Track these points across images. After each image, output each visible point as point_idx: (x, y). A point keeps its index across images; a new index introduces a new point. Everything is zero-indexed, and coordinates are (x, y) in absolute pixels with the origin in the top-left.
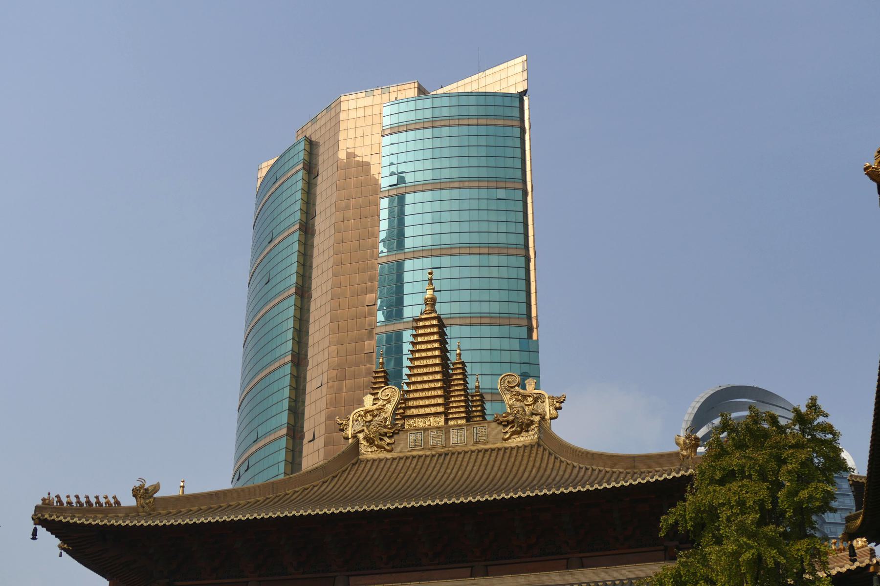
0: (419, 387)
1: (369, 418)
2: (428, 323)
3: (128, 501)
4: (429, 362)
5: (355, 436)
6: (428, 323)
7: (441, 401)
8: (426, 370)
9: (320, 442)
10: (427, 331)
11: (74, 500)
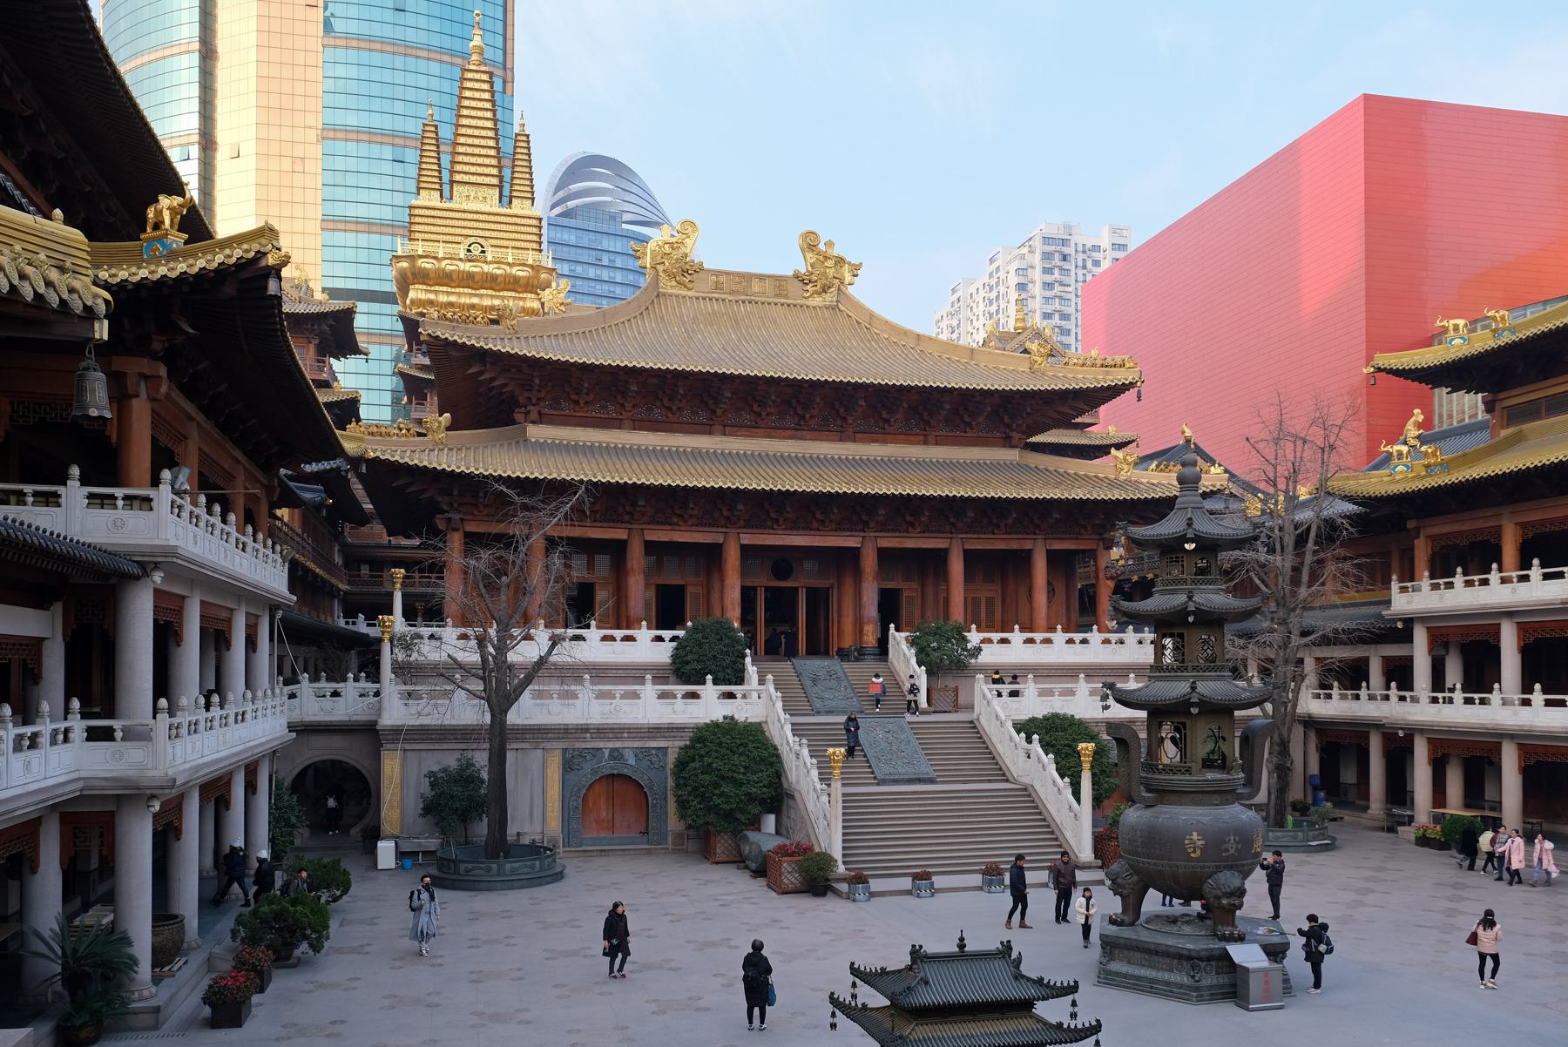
0: (470, 150)
1: (667, 249)
2: (477, 76)
6: (477, 76)
8: (477, 132)
9: (249, 161)
10: (477, 85)
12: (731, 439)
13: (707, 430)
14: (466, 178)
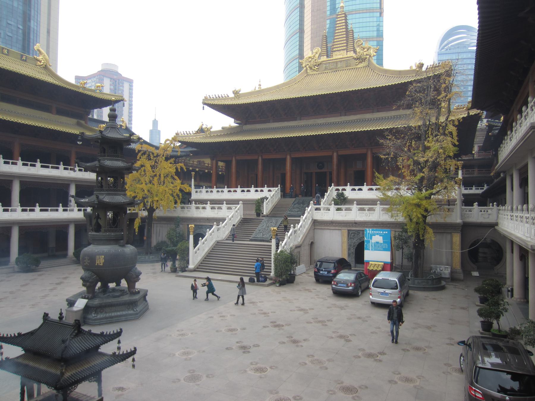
3: (232, 95)
4: (341, 30)
5: (305, 67)
7: (345, 45)
11: (214, 96)
12: (302, 121)
13: (294, 119)
14: (336, 49)
